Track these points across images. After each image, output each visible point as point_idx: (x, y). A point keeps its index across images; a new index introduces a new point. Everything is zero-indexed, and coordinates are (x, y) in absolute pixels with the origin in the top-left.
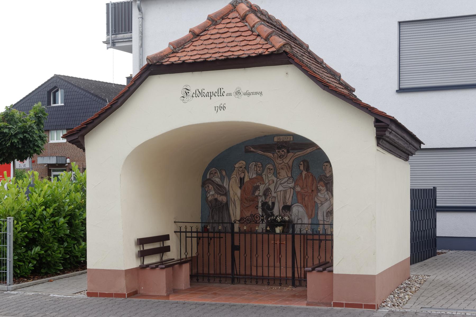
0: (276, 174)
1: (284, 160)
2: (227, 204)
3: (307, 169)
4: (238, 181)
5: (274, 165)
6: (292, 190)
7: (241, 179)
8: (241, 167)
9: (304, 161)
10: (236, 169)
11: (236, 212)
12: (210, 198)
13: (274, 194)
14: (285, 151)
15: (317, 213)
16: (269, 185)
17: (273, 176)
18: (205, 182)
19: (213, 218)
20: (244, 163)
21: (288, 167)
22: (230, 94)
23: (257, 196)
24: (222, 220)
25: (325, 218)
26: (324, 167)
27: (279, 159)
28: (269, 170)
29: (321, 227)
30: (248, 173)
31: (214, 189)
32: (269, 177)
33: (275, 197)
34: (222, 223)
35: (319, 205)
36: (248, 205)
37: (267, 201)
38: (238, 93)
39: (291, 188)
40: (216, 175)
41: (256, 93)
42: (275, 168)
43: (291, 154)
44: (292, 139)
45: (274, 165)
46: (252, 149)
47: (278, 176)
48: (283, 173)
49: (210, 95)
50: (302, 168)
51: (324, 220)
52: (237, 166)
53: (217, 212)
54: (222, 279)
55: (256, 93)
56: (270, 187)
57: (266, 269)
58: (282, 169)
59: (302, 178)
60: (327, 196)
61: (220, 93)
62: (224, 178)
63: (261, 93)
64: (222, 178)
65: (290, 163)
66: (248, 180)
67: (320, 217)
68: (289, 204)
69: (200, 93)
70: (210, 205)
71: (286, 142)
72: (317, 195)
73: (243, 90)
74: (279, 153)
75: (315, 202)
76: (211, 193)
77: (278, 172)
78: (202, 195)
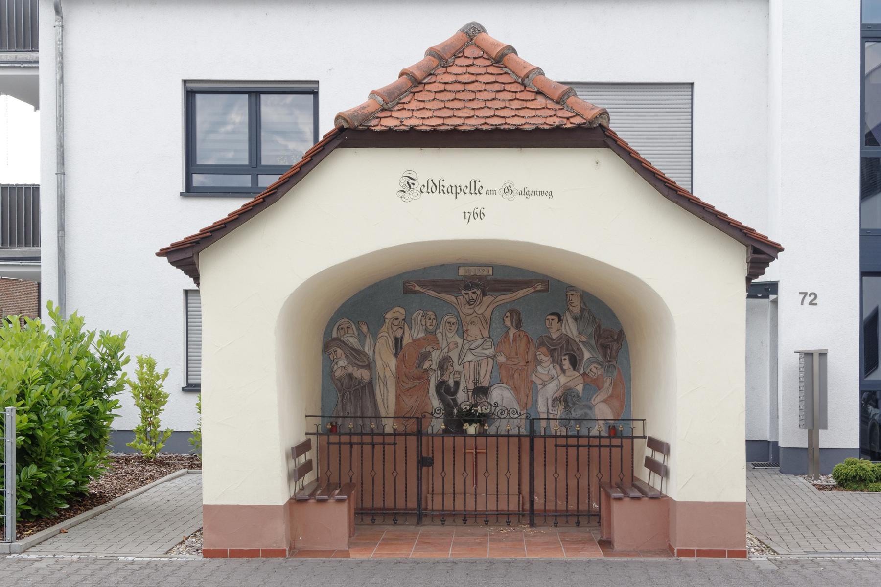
0: (462, 332)
1: (476, 309)
2: (371, 383)
3: (518, 325)
4: (391, 343)
5: (458, 317)
6: (491, 360)
7: (396, 339)
8: (397, 319)
9: (512, 311)
10: (387, 321)
11: (387, 399)
12: (338, 373)
13: (457, 368)
14: (479, 292)
15: (537, 401)
16: (449, 351)
17: (456, 336)
18: (330, 344)
19: (344, 408)
20: (402, 311)
21: (483, 321)
22: (493, 192)
23: (426, 371)
24: (362, 413)
25: (550, 408)
26: (547, 322)
27: (467, 306)
28: (448, 325)
29: (543, 423)
30: (410, 329)
31: (346, 355)
32: (449, 338)
33: (459, 373)
34: (362, 417)
35: (540, 387)
36: (410, 386)
37: (445, 378)
38: (508, 190)
39: (488, 357)
40: (350, 331)
41: (541, 193)
42: (460, 323)
43: (488, 299)
44: (491, 273)
45: (458, 317)
46: (417, 288)
47: (465, 335)
48: (474, 331)
49: (456, 191)
50: (508, 322)
51: (548, 413)
52: (389, 316)
53: (352, 398)
54: (375, 517)
55: (541, 193)
56: (450, 354)
57: (449, 498)
58: (473, 323)
59: (509, 340)
60: (553, 372)
61: (474, 188)
62: (366, 336)
63: (550, 194)
64: (361, 337)
65: (488, 314)
66: (411, 341)
67: (542, 408)
68: (485, 384)
69: (436, 187)
70: (339, 384)
71: (480, 278)
72: (535, 370)
73: (518, 187)
74: (467, 296)
75: (532, 381)
76: (341, 364)
77: (465, 329)
78: (324, 367)
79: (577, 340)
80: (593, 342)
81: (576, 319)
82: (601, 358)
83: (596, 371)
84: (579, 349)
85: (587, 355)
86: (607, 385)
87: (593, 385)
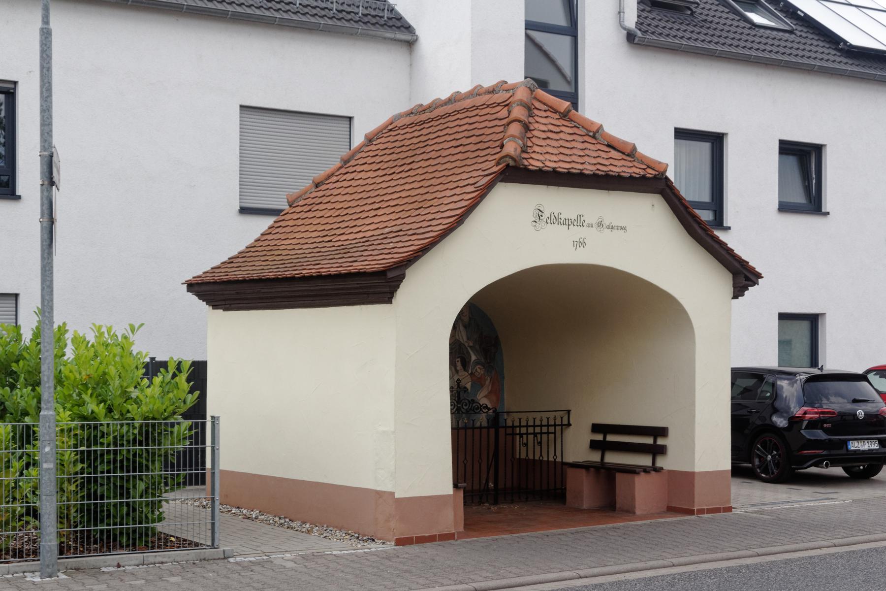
22: (590, 226)
38: (600, 224)
41: (620, 228)
49: (568, 223)
55: (620, 228)
61: (579, 222)
63: (625, 229)
69: (555, 219)
73: (606, 223)
79: (466, 345)
80: (477, 347)
81: (465, 327)
82: (483, 360)
83: (479, 371)
84: (468, 352)
85: (473, 358)
86: (487, 382)
87: (478, 383)
